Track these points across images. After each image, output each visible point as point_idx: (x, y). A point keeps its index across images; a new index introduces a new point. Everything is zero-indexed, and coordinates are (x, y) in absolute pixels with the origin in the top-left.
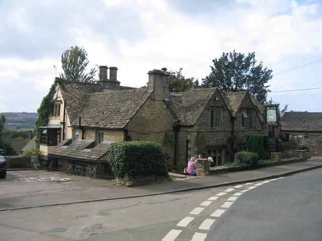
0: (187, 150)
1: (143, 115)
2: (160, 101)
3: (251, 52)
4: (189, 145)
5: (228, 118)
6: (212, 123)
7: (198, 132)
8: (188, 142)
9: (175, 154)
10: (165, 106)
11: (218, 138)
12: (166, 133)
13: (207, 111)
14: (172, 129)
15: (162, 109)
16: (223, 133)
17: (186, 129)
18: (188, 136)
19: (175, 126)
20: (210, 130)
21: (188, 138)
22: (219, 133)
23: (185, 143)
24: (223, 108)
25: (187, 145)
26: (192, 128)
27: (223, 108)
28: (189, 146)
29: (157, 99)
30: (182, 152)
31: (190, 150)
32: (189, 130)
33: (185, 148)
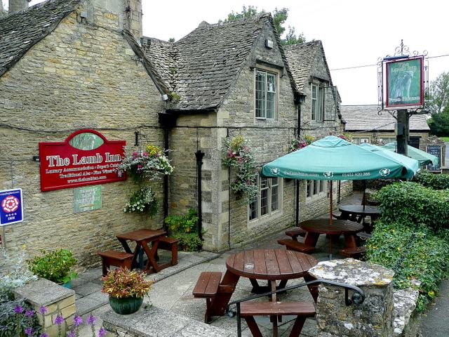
0: (200, 178)
1: (50, 69)
2: (113, 31)
3: (280, 9)
4: (205, 167)
5: (290, 95)
6: (258, 104)
7: (228, 128)
8: (200, 156)
9: (166, 192)
10: (130, 52)
11: (272, 144)
12: (137, 134)
13: (247, 72)
14: (154, 121)
15: (121, 60)
16: (280, 132)
17: (193, 121)
18: (202, 140)
19: (163, 112)
20: (255, 124)
21: (202, 146)
22: (273, 131)
23: (193, 161)
24: (281, 68)
25: (199, 163)
26: (211, 117)
27: (281, 68)
28: (205, 167)
29: (101, 21)
30: (185, 186)
31: (209, 178)
32: (204, 122)
33: (194, 174)
